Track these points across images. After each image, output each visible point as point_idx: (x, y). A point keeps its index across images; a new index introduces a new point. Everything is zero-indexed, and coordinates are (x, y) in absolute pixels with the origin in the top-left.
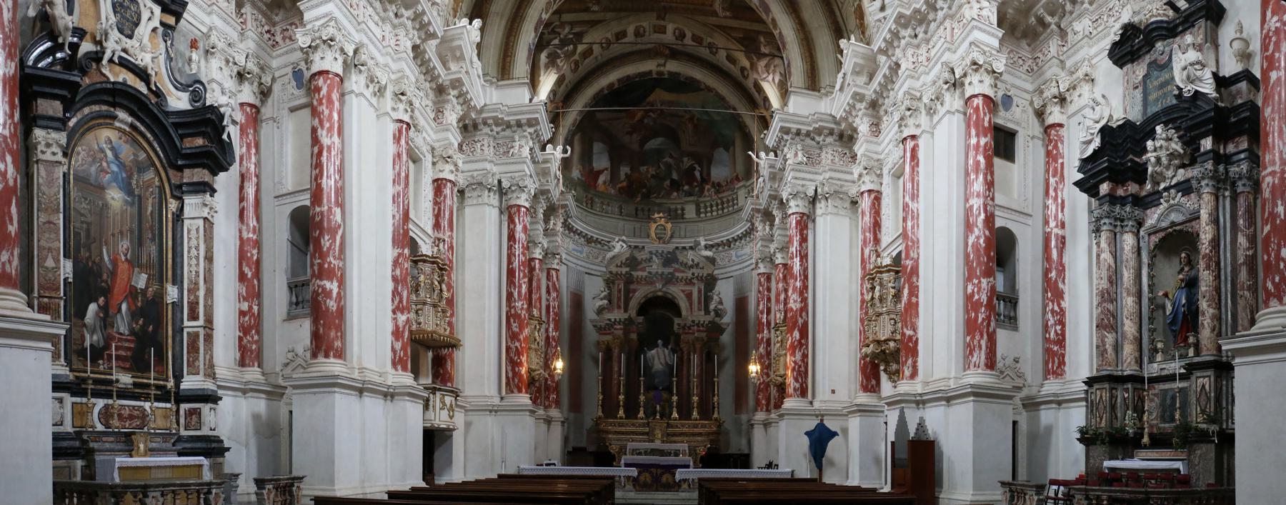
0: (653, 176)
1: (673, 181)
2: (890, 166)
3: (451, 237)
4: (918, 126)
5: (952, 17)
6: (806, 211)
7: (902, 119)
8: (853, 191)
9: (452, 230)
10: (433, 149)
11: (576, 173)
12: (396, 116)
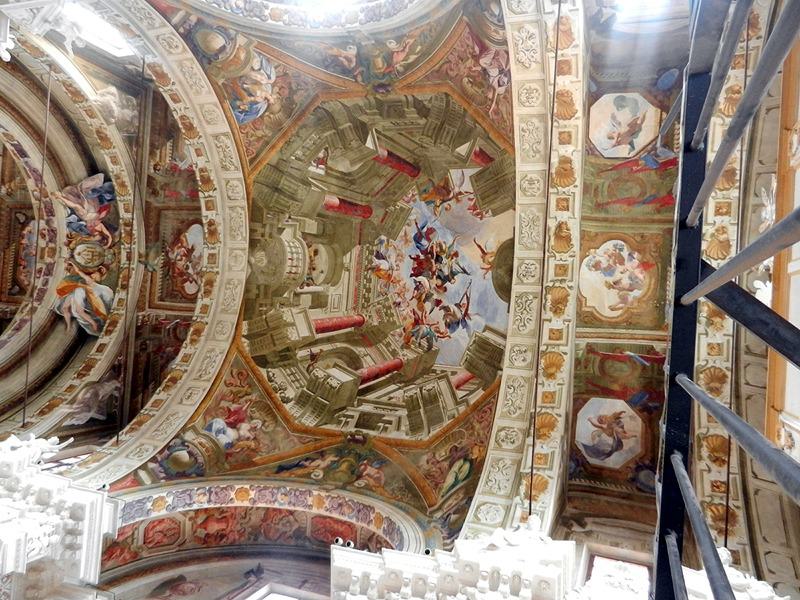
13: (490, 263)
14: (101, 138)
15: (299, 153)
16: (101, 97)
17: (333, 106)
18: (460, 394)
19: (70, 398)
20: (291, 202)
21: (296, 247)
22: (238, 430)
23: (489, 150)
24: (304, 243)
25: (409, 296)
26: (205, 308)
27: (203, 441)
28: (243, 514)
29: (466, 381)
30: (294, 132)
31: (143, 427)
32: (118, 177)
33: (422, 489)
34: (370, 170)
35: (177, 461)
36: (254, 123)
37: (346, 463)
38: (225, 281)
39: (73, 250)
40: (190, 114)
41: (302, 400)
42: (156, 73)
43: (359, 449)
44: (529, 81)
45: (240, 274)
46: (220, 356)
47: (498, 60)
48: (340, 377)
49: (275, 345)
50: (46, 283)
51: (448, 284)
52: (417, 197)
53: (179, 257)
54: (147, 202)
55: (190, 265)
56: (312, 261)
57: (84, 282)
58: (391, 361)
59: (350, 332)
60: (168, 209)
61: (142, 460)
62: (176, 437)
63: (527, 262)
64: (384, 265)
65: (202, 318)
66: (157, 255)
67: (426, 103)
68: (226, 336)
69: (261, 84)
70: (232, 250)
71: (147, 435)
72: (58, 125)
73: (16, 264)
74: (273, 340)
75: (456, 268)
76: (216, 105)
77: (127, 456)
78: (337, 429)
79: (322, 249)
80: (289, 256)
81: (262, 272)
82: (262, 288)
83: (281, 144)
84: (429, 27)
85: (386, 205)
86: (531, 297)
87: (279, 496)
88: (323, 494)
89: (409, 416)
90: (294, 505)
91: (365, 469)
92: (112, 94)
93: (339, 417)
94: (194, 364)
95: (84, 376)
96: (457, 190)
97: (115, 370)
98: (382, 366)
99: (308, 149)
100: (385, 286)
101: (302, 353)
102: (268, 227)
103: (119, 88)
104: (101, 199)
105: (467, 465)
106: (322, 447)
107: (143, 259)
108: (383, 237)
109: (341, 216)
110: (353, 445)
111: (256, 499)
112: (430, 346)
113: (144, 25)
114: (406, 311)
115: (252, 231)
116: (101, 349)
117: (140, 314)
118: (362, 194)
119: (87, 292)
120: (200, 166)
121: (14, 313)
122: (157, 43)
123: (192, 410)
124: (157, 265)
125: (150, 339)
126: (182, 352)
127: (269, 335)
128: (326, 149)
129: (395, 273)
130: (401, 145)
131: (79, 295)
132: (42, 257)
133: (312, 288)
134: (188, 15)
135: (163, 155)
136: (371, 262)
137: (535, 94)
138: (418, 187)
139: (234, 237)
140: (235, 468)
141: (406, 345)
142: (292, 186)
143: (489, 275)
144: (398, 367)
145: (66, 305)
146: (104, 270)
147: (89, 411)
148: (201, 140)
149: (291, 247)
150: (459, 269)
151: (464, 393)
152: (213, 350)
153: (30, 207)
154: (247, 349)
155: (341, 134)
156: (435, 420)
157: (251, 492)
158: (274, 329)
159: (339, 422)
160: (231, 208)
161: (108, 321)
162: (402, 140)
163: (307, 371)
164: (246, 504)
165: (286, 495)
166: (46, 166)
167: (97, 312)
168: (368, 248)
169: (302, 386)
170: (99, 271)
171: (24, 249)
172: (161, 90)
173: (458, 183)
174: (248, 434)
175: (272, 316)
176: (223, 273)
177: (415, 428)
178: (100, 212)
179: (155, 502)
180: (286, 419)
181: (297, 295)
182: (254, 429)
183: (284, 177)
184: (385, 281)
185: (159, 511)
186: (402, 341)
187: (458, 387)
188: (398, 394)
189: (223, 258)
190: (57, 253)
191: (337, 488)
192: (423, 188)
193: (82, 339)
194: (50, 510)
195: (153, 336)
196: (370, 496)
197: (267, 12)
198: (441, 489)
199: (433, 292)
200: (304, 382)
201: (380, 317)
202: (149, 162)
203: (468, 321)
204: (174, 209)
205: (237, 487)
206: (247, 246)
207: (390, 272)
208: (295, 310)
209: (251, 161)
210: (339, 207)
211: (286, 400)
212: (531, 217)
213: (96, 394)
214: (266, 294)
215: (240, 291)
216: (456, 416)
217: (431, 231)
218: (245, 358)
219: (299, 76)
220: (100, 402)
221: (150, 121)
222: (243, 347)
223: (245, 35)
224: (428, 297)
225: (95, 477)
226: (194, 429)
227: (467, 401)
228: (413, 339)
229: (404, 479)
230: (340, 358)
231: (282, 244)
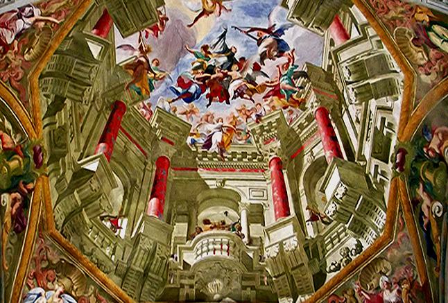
15: (108, 251)
20: (157, 256)
24: (197, 237)
25: (249, 105)
34: (120, 164)
41: (359, 229)
48: (334, 185)
51: (237, 57)
52: (146, 103)
56: (215, 226)
58: (318, 123)
64: (217, 137)
75: (219, 48)
79: (203, 215)
98: (323, 134)
100: (239, 134)
101: (311, 233)
102: (183, 281)
105: (437, 28)
109: (168, 194)
112: (303, 74)
114: (266, 106)
118: (144, 171)
128: (102, 218)
129: (226, 124)
130: (93, 127)
138: (135, 102)
141: (301, 104)
142: (141, 256)
144: (323, 112)
149: (202, 253)
155: (87, 202)
162: (88, 126)
163: (329, 224)
169: (344, 230)
177: (389, 89)
181: (250, 243)
183: (132, 266)
184: (235, 135)
186: (297, 110)
188: (354, 110)
200: (340, 228)
208: (266, 244)
217: (181, 82)
228: (294, 96)
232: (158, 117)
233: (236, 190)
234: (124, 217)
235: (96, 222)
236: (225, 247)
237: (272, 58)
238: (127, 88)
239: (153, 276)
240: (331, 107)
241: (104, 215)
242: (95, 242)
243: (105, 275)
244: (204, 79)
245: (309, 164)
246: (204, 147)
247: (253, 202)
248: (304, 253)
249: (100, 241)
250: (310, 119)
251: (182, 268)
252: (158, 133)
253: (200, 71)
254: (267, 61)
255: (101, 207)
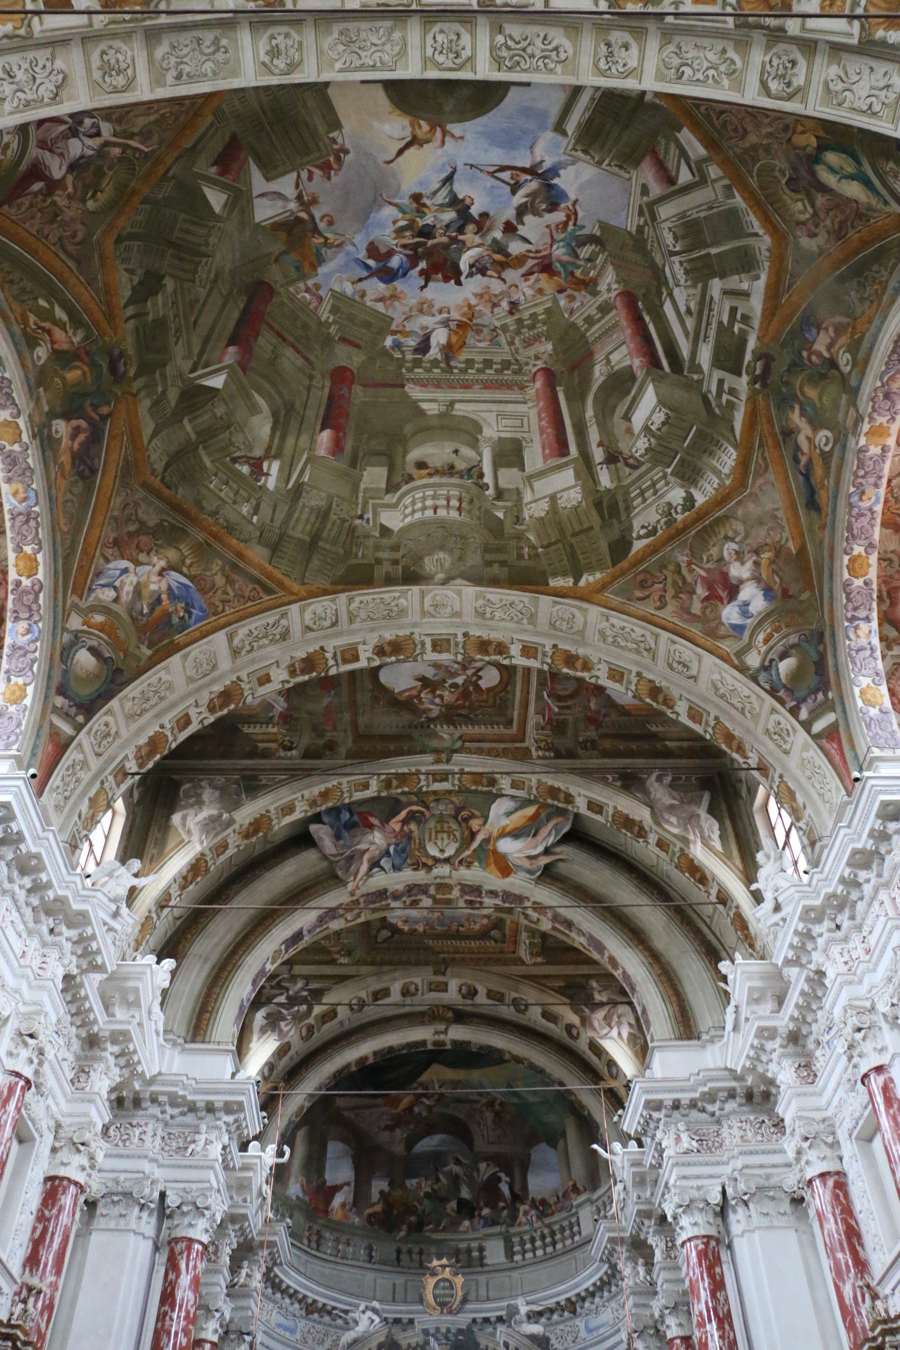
0: (428, 1195)
1: (462, 1203)
2: (848, 1124)
3: (54, 1286)
4: (882, 1050)
5: (887, 885)
6: (713, 1232)
7: (851, 1047)
8: (790, 1181)
9: (58, 1273)
10: (58, 1126)
11: (294, 1189)
12: (10, 1064)
13: (432, 129)
14: (256, 832)
15: (245, 509)
16: (192, 839)
17: (157, 454)
18: (685, 176)
19: (679, 845)
20: (333, 517)
21: (413, 503)
22: (741, 582)
23: (216, 146)
24: (405, 488)
25: (496, 286)
26: (528, 651)
27: (761, 637)
28: (884, 564)
29: (661, 167)
30: (210, 520)
31: (736, 733)
32: (313, 803)
33: (865, 244)
35: (797, 675)
36: (203, 591)
37: (806, 389)
38: (480, 620)
39: (437, 861)
40: (205, 698)
41: (689, 475)
42: (151, 754)
43: (780, 367)
44: (89, 69)
45: (466, 597)
46: (612, 620)
47: (55, 141)
48: (647, 408)
49: (591, 528)
50: (493, 893)
51: (475, 211)
52: (310, 283)
53: (437, 700)
54: (347, 758)
55: (450, 682)
57: (487, 841)
58: (619, 315)
59: (566, 394)
60: (355, 725)
61: (794, 730)
62: (755, 679)
63: (429, 52)
64: (440, 337)
65: (544, 654)
66: (435, 735)
67: (136, 280)
68: (575, 611)
69: (138, 583)
70: (423, 613)
71: (750, 724)
72: (244, 893)
73: (458, 936)
74: (582, 532)
76: (185, 657)
77: (787, 752)
78: (743, 409)
79: (415, 454)
80: (429, 513)
81: (461, 558)
82: (489, 557)
83: (234, 542)
84: (7, 286)
85: (328, 341)
86: (500, 39)
87: (865, 504)
88: (866, 427)
89: (723, 276)
90: (880, 478)
91: (819, 355)
92: (184, 818)
93: (720, 406)
94: (627, 661)
95: (642, 828)
96: (293, 206)
97: (630, 782)
98: (628, 332)
99: (237, 493)
101: (605, 480)
102: (380, 554)
103: (172, 811)
104: (351, 826)
106: (773, 435)
107: (444, 756)
108: (388, 342)
110: (773, 378)
111: (866, 543)
113: (86, 777)
114: (525, 289)
115: (389, 581)
116: (594, 806)
117: (534, 753)
119: (503, 834)
120: (285, 676)
121: (532, 932)
122: (105, 756)
123: (709, 660)
124: (451, 735)
125: (576, 736)
126: (604, 682)
127: (573, 540)
128: (235, 460)
129: (455, 315)
130: (215, 323)
131: (507, 846)
132: (448, 902)
133: (487, 468)
134: (55, 710)
135: (265, 737)
136: (435, 363)
137: (111, 56)
138: (292, 282)
139: (402, 612)
140: (809, 586)
141: (589, 285)
142: (304, 516)
143: (455, 128)
144: (629, 298)
145: (526, 864)
146: (464, 814)
147: (699, 816)
148: (245, 678)
149: (413, 512)
150: (444, 192)
151: (684, 169)
152: (602, 633)
153: (367, 924)
154: (598, 575)
155: (206, 435)
156: (731, 222)
157: (855, 553)
158: (561, 531)
159: (731, 406)
160: (351, 620)
161: (549, 801)
162: (206, 320)
163: (634, 467)
164: (873, 559)
165: (863, 493)
166: (312, 904)
167: (533, 818)
168: (410, 370)
169: (665, 476)
170: (466, 820)
171: (432, 928)
172: (174, 746)
173: (280, 203)
174: (749, 564)
175: (538, 536)
176: (467, 624)
177: (745, 263)
178: (371, 826)
179: (868, 703)
180: (722, 499)
181: (500, 494)
182: (739, 556)
183: (291, 533)
184: (470, 334)
185: (882, 696)
186: (582, 296)
187: (671, 180)
188: (683, 295)
189: (441, 627)
190: (446, 881)
191: (855, 405)
192: (293, 273)
193: (578, 836)
194: (883, 850)
195: (570, 732)
196: (871, 349)
197: (26, 582)
198: (870, 208)
199: (489, 239)
200: (657, 473)
201: (537, 339)
202: (280, 758)
203: (546, 165)
204: (355, 714)
205: (846, 575)
206: (415, 590)
207: (453, 325)
208: (527, 497)
209: (269, 591)
210: (338, 429)
211: (689, 501)
212: (341, 48)
213: (671, 808)
214: (499, 550)
215: (495, 595)
216: (726, 182)
217: (373, 250)
218: (614, 578)
219: (115, 519)
220: (682, 802)
221: (213, 762)
222: (597, 582)
223: (66, 618)
224: (499, 247)
225: (821, 795)
226: (740, 654)
227: (701, 162)
228: (578, 273)
229: (842, 279)
230: (613, 412)
231: (411, 526)
232: (333, 306)
233: (472, 416)
234: (275, 457)
235: (224, 465)
236: (454, 503)
237: (537, 213)
238: (277, 260)
239: (328, 547)
240: (643, 291)
241: (237, 454)
242: (222, 495)
243: (242, 545)
244: (414, 247)
245: (602, 378)
246: (416, 350)
247: (503, 435)
248: (594, 512)
249: (231, 495)
250: (605, 309)
251: (377, 534)
252: (332, 330)
253: (408, 233)
254: (529, 219)
255: (232, 444)
